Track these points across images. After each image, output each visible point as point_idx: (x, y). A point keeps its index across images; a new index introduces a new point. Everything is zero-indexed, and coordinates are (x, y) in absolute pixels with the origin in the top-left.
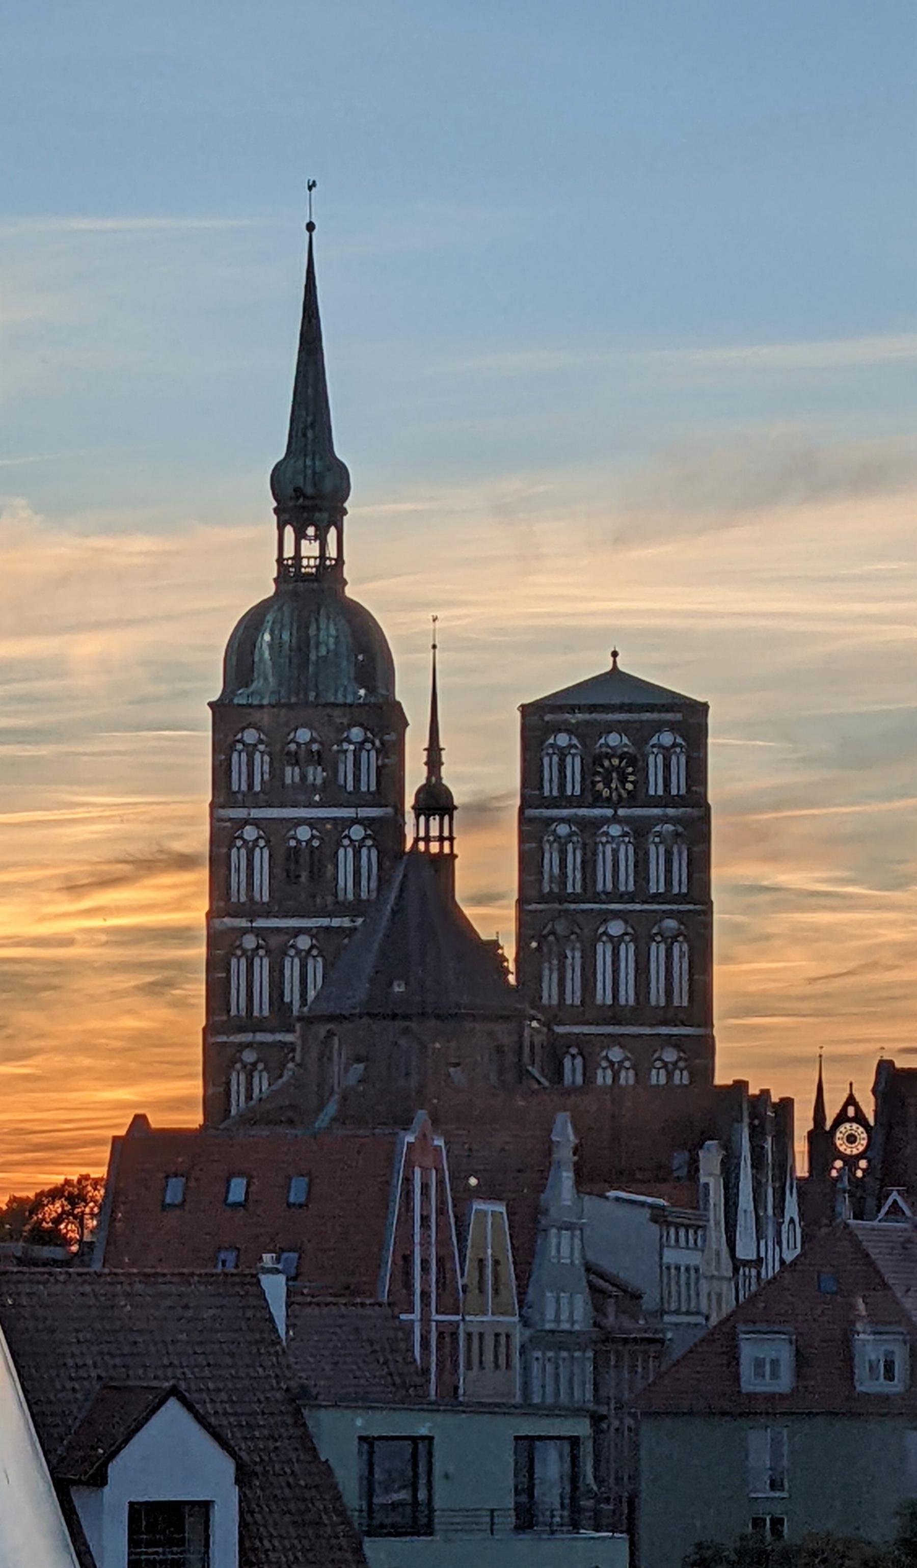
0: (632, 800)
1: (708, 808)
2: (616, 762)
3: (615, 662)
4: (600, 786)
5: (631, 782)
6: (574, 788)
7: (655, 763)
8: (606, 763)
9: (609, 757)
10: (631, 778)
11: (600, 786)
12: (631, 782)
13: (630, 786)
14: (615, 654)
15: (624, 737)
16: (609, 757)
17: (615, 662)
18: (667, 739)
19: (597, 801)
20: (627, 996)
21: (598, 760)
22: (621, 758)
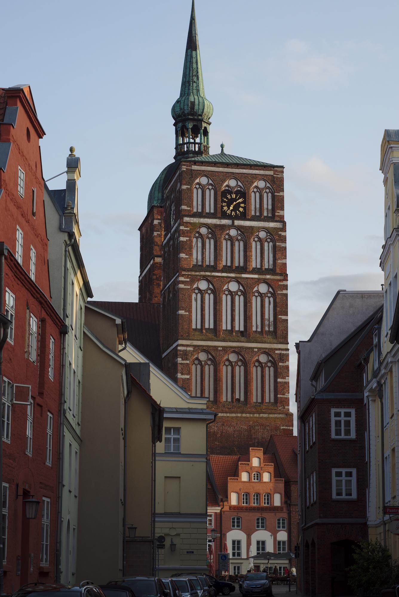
0: (244, 216)
1: (284, 223)
2: (234, 196)
3: (222, 150)
4: (225, 208)
5: (242, 207)
6: (210, 208)
7: (254, 199)
8: (229, 197)
9: (230, 193)
10: (242, 205)
11: (225, 208)
12: (242, 207)
13: (241, 209)
14: (222, 146)
15: (239, 182)
16: (230, 193)
17: (222, 150)
18: (261, 184)
19: (224, 216)
20: (239, 326)
21: (225, 193)
22: (237, 193)
